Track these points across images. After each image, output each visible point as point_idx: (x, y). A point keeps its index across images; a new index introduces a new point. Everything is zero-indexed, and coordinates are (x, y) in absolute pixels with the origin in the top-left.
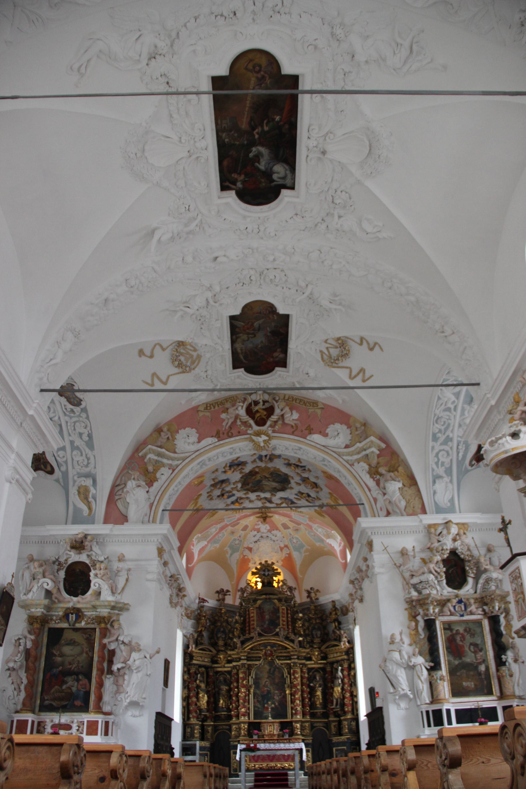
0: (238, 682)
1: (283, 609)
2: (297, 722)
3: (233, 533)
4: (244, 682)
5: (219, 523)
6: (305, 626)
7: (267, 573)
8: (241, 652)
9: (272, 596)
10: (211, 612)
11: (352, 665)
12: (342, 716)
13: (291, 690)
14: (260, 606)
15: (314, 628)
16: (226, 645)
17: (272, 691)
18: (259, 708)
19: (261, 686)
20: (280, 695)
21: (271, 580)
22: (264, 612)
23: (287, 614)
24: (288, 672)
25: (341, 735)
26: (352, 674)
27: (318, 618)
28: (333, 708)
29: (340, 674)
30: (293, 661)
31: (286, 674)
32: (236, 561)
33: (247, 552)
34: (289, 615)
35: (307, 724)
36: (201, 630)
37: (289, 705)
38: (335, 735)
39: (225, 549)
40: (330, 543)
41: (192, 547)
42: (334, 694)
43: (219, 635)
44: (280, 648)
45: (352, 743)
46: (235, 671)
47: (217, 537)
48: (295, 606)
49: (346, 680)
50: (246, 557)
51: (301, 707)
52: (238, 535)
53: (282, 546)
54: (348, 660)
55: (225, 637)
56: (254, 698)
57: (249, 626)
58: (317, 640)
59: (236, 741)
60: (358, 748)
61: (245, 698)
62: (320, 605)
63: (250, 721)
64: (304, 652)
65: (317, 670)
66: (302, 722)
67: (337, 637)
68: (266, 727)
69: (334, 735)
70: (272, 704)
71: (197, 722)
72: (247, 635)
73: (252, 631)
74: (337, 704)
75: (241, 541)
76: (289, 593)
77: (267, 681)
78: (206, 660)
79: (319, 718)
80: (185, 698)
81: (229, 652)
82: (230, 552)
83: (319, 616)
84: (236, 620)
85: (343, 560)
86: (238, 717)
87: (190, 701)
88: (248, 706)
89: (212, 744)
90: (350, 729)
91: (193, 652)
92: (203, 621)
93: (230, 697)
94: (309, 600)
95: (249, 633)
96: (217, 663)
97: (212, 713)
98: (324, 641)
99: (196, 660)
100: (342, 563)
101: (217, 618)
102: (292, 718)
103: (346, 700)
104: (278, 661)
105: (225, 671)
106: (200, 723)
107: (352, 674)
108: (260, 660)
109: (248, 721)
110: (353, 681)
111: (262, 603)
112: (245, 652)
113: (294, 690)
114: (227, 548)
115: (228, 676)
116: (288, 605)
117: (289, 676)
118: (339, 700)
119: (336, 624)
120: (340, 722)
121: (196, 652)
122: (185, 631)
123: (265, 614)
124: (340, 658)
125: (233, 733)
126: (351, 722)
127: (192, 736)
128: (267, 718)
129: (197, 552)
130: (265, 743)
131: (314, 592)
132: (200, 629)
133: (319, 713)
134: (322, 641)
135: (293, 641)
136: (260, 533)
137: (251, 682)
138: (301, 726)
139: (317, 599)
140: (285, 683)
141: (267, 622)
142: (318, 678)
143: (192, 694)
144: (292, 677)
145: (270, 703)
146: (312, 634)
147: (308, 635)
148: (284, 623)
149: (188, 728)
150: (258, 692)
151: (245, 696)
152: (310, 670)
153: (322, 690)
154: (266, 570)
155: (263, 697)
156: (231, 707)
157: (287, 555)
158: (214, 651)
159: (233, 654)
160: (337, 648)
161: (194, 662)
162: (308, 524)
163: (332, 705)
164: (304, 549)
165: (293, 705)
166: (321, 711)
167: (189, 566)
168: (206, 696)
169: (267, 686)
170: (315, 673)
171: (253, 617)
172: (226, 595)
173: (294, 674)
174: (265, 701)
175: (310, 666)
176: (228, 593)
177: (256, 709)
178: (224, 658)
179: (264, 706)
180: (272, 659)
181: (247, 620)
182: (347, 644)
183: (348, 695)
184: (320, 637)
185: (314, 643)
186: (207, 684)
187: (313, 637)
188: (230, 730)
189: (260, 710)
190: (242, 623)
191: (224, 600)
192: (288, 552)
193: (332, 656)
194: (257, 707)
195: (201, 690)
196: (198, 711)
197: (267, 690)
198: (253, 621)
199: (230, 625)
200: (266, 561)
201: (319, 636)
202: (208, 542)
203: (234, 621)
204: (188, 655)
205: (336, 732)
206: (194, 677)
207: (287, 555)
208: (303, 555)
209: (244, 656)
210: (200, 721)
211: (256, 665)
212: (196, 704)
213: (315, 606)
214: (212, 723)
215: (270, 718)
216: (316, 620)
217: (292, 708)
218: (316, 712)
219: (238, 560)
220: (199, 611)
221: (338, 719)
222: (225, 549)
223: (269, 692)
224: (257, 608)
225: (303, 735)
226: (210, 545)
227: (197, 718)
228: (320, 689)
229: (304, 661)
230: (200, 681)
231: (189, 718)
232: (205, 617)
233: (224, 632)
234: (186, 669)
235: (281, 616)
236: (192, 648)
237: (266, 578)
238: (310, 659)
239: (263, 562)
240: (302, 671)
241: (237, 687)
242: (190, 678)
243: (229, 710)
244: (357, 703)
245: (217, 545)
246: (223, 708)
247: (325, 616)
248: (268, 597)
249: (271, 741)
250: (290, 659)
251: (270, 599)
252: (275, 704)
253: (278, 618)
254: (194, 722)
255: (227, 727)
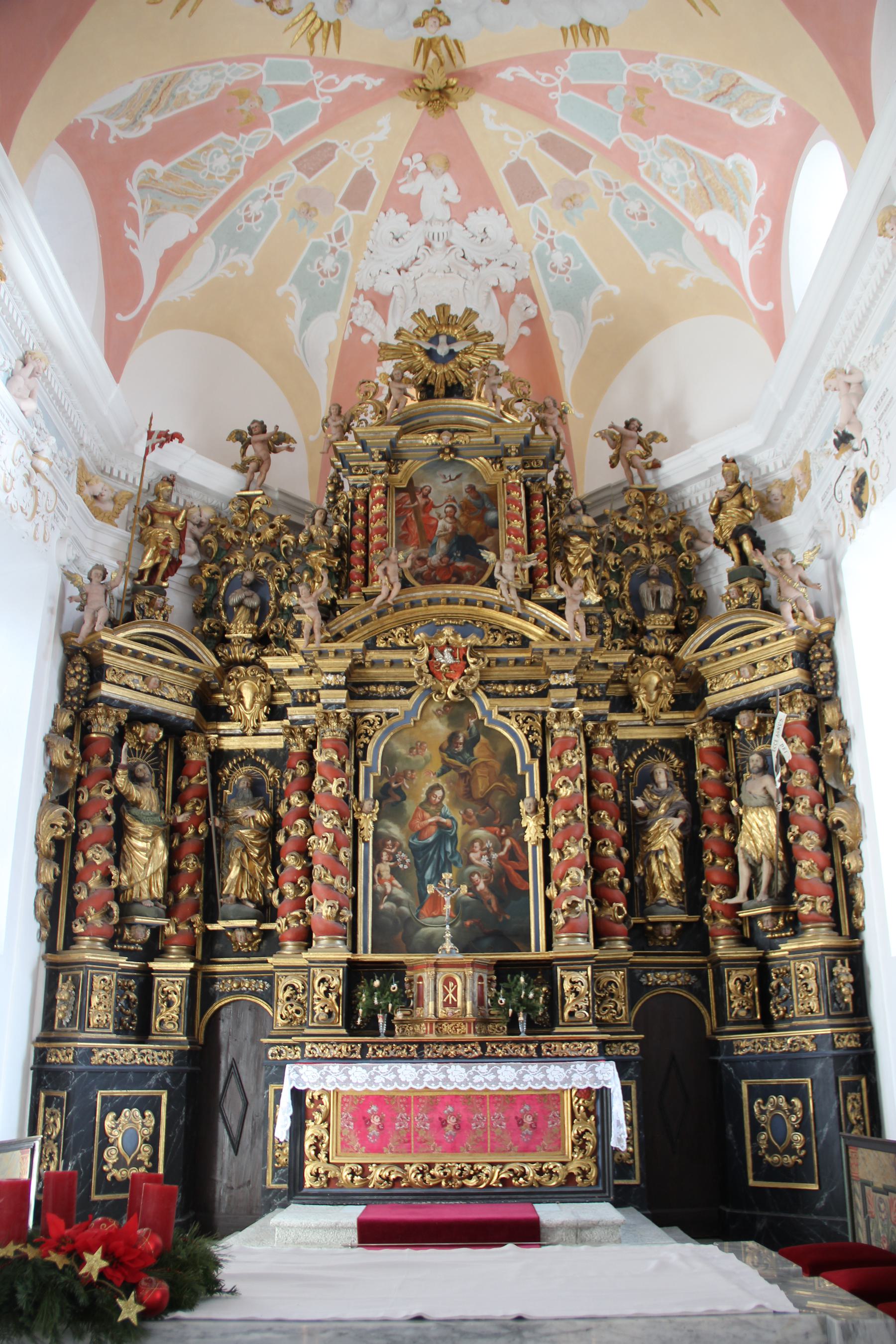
0: (311, 796)
1: (514, 487)
2: (574, 963)
3: (308, 211)
4: (333, 787)
5: (247, 131)
6: (606, 564)
7: (442, 350)
8: (321, 653)
9: (462, 439)
10: (207, 514)
11: (829, 715)
12: (784, 940)
13: (545, 828)
14: (411, 482)
15: (647, 576)
16: (262, 640)
17: (461, 830)
18: (398, 902)
19: (410, 806)
20: (498, 849)
21: (461, 375)
22: (429, 506)
23: (530, 514)
24: (531, 745)
25: (768, 1023)
26: (836, 747)
27: (662, 537)
28: (739, 907)
29: (778, 745)
30: (555, 696)
31: (524, 758)
32: (326, 352)
33: (365, 313)
34: (538, 518)
35: (619, 977)
36: (155, 569)
37: (536, 890)
38: (747, 1024)
39: (280, 291)
40: (709, 232)
41: (130, 234)
42: (744, 843)
43: (234, 600)
44: (500, 640)
45: (839, 1060)
46: (299, 746)
47: (236, 208)
48: (561, 490)
49: (802, 778)
50: (365, 338)
51: (589, 897)
52: (332, 232)
53: (508, 285)
54: (811, 690)
55: (263, 608)
56: (377, 859)
57: (366, 560)
58: (658, 622)
59: (290, 1045)
60: (863, 1082)
61: (336, 856)
62: (670, 491)
63: (361, 956)
64: (605, 666)
65: (655, 750)
66: (600, 965)
67: (752, 599)
68: (427, 985)
69: (739, 1021)
70: (459, 881)
71: (109, 958)
72: (355, 595)
73: (378, 571)
74: (750, 894)
75: (343, 259)
76: (539, 431)
77: (437, 787)
78: (173, 693)
79: (668, 948)
80: (58, 843)
81: (271, 662)
82: (300, 307)
83: (663, 530)
84: (311, 538)
85: (764, 303)
86: (306, 939)
87: (80, 865)
88: (351, 892)
89: (179, 1056)
90: (832, 998)
91: (105, 645)
92: (164, 530)
93: (275, 859)
94: (618, 474)
95: (366, 584)
96: (228, 718)
97: (191, 924)
98: (682, 631)
99: (113, 683)
100: (759, 313)
101: (229, 534)
102: (549, 947)
103: (806, 864)
104: (486, 702)
105: (258, 752)
106: (123, 962)
107: (836, 747)
108: (408, 697)
109: (348, 955)
110: (832, 783)
111: (423, 468)
112: (337, 653)
113: (560, 821)
114: (286, 288)
115: (271, 771)
116: (533, 480)
117: (536, 764)
118: (765, 871)
119: (747, 547)
120: (763, 968)
121: (120, 649)
122: (65, 554)
123: (433, 513)
124: (767, 685)
125: (281, 1010)
126: (833, 964)
127: (80, 1017)
128: (431, 946)
129: (156, 265)
130: (421, 1058)
131: (640, 442)
132: (148, 563)
133: (667, 930)
134: (676, 623)
135: (557, 607)
136: (419, 227)
137: (367, 790)
138: (595, 982)
139: (656, 465)
140: (523, 796)
141: (442, 545)
142: (662, 778)
143: (86, 833)
144: (553, 767)
145: (447, 876)
146: (636, 598)
147: (620, 604)
148: (519, 542)
149: (65, 980)
150: (395, 830)
151: (337, 844)
152: (623, 749)
153: (682, 827)
154: (443, 339)
155: (419, 853)
156: (275, 896)
157: (526, 331)
158: (209, 660)
159: (291, 672)
160: (760, 635)
161: (106, 689)
162: (620, 144)
163: (733, 893)
164: (595, 297)
165: (552, 892)
166: (684, 917)
167: (119, 317)
168: (161, 843)
169: (439, 805)
170: (651, 760)
171: (379, 516)
172: (275, 452)
173: (559, 759)
174: (428, 874)
175: (622, 734)
176: (284, 445)
177: (386, 905)
178: (255, 695)
179: (422, 896)
180: (459, 691)
181: (360, 537)
182: (810, 612)
183: (810, 841)
184: (670, 611)
185: (645, 632)
186: (178, 797)
187: (641, 612)
188: (269, 997)
189: (405, 909)
190: (338, 553)
191: (262, 465)
192: (532, 312)
193: (730, 680)
194: (392, 898)
195: (137, 818)
196: (115, 907)
197: (439, 824)
198: (383, 532)
199: (286, 562)
200: (443, 309)
201: (665, 602)
202: (204, 223)
203: (302, 538)
204: (80, 659)
205: (752, 1011)
206: (106, 760)
207: (526, 331)
208: (591, 325)
209: (335, 674)
210: (132, 956)
211: (389, 716)
212: (107, 878)
213: (648, 492)
214: (189, 966)
215: (448, 946)
216: (648, 542)
217: (548, 902)
218: (655, 924)
219: (331, 346)
220: (152, 499)
221: (760, 953)
222: (280, 291)
223: (444, 833)
224: (399, 491)
225: (599, 1023)
226: (207, 239)
227: (114, 941)
228: (678, 821)
229: (603, 707)
230: (134, 778)
231: (71, 939)
232: (174, 516)
233: (256, 585)
234: (66, 720)
235: (502, 520)
236: (94, 620)
237: (440, 370)
238: (626, 703)
239: (431, 312)
240: (590, 751)
241: (305, 814)
242: (86, 759)
243: (266, 912)
244: (850, 879)
245: (248, 262)
246: (238, 900)
247: (685, 530)
248: (446, 438)
249: (452, 1051)
250: (543, 694)
251: (453, 449)
252: (472, 888)
253: (495, 525)
254: (88, 957)
255: (261, 985)
